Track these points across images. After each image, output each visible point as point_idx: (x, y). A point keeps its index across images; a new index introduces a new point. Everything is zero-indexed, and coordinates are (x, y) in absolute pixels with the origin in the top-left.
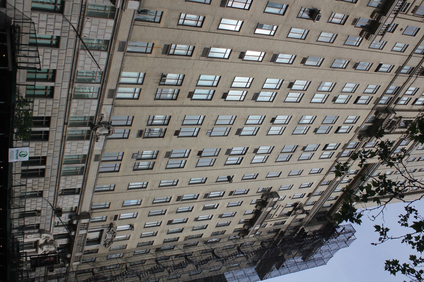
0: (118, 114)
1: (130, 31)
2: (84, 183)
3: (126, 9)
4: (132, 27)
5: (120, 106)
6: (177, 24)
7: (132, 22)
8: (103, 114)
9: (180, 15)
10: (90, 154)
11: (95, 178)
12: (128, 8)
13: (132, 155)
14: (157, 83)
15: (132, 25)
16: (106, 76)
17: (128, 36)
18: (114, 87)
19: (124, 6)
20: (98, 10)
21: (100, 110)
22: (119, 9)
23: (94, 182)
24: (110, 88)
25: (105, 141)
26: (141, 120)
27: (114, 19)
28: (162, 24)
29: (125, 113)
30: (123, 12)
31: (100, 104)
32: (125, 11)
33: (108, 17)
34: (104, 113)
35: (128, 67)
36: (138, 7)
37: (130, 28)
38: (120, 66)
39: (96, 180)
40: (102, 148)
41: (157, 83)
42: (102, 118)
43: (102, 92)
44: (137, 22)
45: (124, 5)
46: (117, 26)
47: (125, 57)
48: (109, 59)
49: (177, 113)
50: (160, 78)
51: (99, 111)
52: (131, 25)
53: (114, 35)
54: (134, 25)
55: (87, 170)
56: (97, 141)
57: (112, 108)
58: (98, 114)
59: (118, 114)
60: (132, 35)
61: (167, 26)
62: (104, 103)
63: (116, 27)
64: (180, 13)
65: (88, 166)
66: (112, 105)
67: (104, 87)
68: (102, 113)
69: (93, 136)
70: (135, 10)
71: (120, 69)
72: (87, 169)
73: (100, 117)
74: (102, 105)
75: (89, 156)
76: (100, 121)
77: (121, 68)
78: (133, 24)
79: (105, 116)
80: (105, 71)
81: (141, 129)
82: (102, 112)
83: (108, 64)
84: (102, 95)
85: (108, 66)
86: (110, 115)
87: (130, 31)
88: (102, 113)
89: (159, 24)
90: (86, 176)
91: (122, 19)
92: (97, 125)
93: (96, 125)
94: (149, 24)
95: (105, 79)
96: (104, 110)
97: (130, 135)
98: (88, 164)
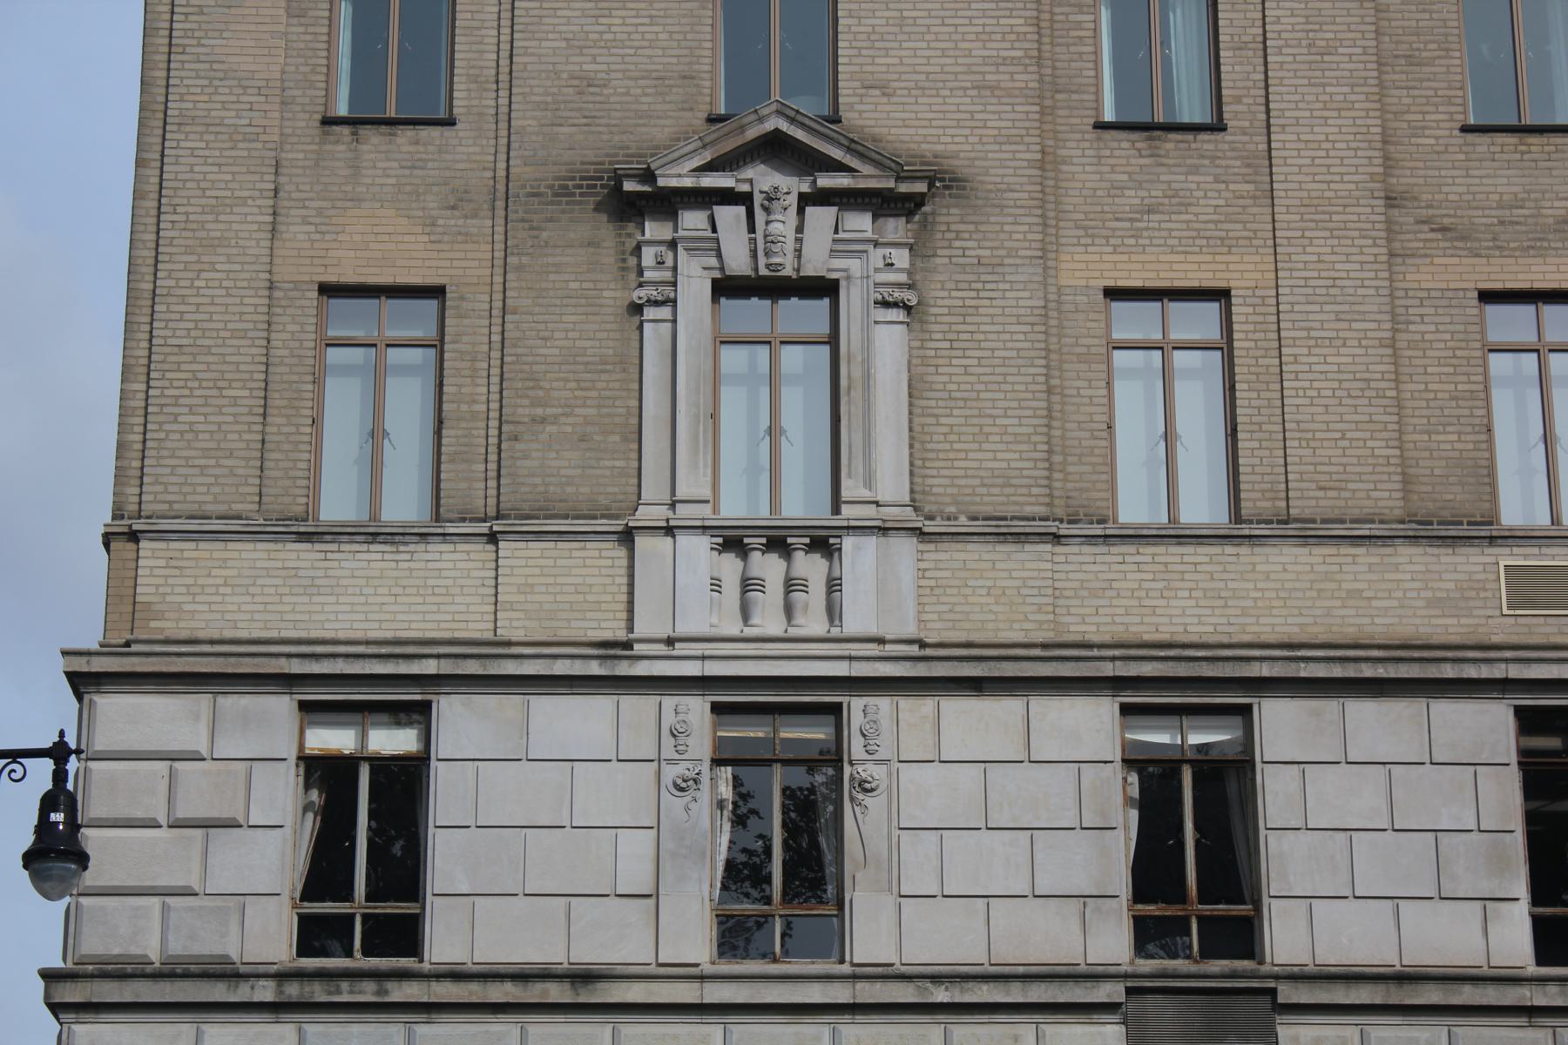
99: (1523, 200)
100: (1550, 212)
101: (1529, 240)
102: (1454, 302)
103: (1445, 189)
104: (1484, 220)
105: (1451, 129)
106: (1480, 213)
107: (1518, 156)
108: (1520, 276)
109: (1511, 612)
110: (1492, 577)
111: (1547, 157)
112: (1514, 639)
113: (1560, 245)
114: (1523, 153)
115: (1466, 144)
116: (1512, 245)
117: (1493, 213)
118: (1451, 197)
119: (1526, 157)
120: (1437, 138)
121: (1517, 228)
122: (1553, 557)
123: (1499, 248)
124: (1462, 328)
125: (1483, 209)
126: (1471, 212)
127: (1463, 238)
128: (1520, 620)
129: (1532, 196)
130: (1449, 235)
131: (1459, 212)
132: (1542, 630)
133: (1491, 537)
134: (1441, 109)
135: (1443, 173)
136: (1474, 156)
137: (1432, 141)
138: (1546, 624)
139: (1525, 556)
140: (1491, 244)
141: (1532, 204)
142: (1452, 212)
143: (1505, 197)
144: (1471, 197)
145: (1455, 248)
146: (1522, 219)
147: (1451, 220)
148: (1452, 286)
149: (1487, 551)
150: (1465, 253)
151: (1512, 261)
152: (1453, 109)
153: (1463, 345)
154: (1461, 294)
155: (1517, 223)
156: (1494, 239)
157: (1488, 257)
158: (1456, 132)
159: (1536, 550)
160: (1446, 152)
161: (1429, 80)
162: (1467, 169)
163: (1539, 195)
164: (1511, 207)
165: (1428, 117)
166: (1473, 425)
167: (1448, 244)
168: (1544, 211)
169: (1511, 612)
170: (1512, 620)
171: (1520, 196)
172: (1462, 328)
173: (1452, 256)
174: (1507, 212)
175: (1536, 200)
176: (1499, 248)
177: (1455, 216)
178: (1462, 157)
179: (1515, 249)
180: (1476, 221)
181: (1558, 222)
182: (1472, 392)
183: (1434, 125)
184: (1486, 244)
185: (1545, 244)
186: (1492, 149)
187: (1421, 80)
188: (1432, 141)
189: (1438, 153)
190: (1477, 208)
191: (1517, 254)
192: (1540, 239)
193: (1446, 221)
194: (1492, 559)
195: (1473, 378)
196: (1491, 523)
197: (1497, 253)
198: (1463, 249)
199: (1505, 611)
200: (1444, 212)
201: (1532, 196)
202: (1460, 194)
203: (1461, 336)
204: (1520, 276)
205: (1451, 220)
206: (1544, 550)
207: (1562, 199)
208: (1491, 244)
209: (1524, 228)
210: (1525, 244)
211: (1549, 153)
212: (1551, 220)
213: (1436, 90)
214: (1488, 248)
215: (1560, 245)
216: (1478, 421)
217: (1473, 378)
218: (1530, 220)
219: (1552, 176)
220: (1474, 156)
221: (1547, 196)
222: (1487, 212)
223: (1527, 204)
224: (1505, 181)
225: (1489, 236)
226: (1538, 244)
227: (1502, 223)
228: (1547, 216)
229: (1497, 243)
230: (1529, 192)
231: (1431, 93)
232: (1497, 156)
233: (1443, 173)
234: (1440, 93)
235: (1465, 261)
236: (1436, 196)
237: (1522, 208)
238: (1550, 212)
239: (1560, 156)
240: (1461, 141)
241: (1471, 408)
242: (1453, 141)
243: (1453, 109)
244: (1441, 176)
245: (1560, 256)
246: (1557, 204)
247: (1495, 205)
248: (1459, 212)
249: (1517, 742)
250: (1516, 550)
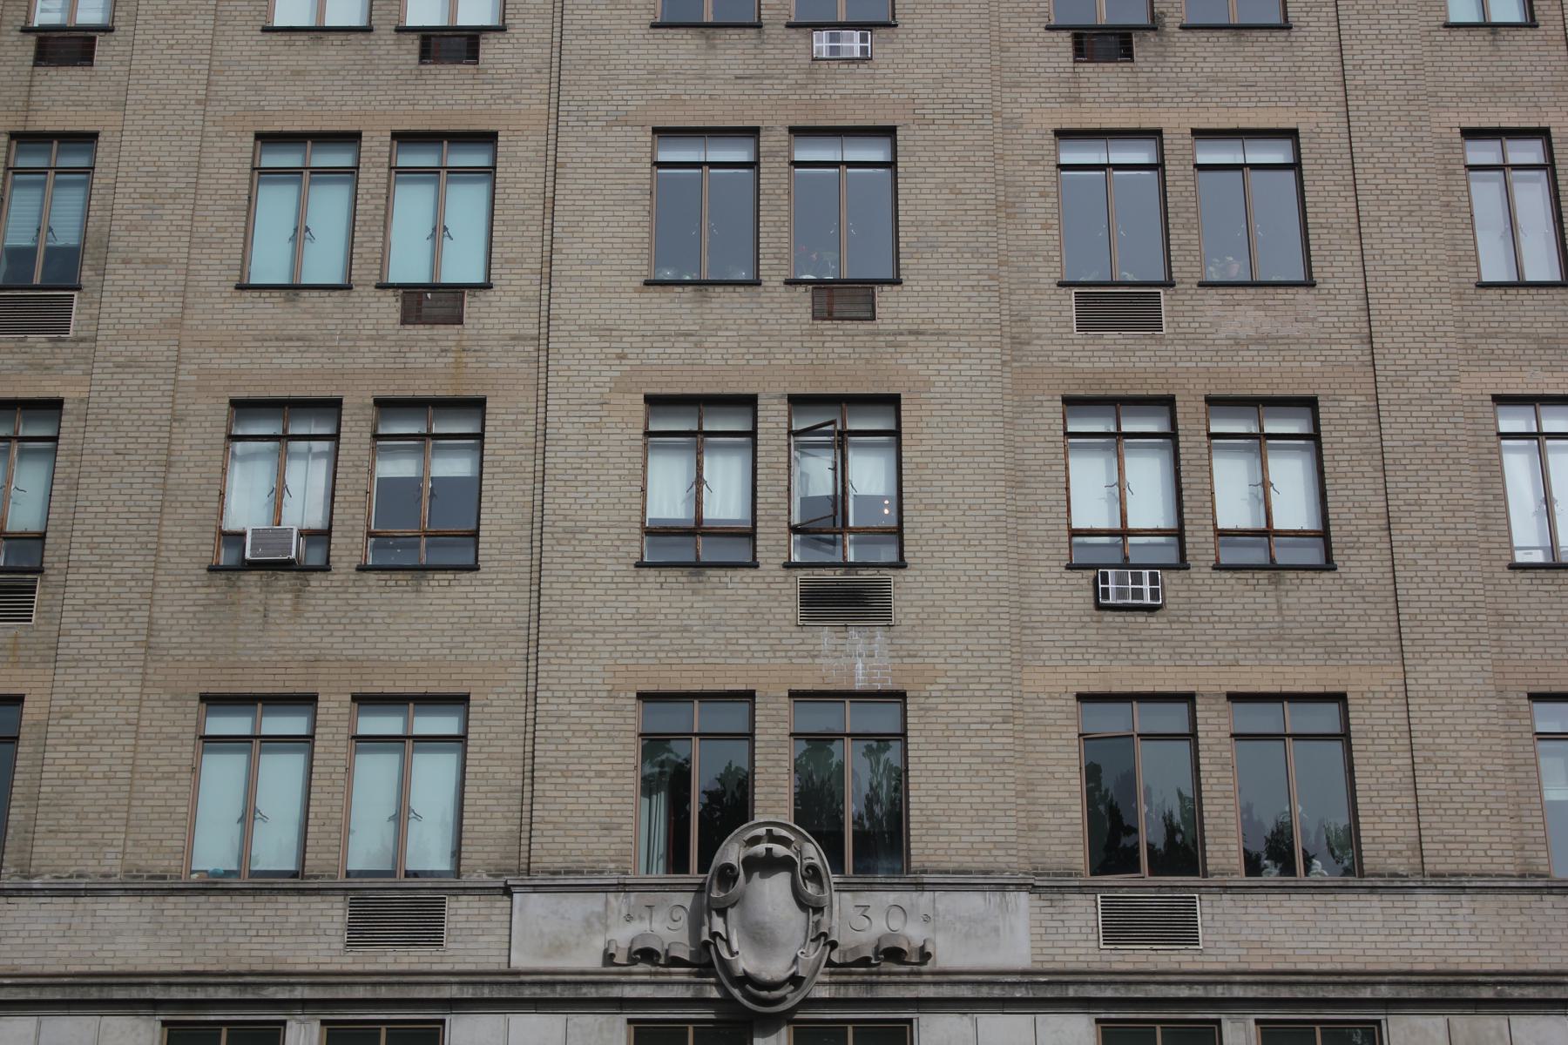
0: (607, 828)
2: (1487, 993)
5: (526, 825)
8: (609, 958)
10: (1071, 992)
11: (1427, 904)
13: (1109, 617)
14: (298, 593)
16: (200, 994)
18: (334, 914)
21: (580, 979)
23: (1490, 902)
24: (338, 939)
25: (920, 887)
26: (686, 629)
29: (600, 774)
31: (486, 993)
34: (599, 944)
35: (136, 843)
38: (124, 903)
39: (1452, 885)
40: (1023, 898)
41: (298, 593)
42: (648, 955)
43: (360, 993)
47: (36, 883)
48: (33, 994)
49: (622, 357)
50: (252, 577)
51: (559, 992)
55: (1199, 992)
56: (925, 956)
57: (536, 889)
58: (592, 992)
59: (607, 828)
62: (494, 962)
65: (1238, 992)
66: (507, 891)
67: (299, 993)
68: (592, 961)
69: (852, 993)
71: (149, 901)
72: (1285, 993)
73: (642, 967)
74: (513, 977)
75: (1109, 993)
76: (676, 962)
77: (141, 892)
79: (624, 935)
80: (154, 1005)
81: (790, 607)
82: (588, 959)
83: (77, 994)
84: (384, 993)
85: (94, 994)
86: (622, 888)
88: (592, 961)
90: (1385, 992)
92: (719, 985)
93: (714, 993)
95: (224, 993)
96: (559, 948)
97: (859, 685)
98: (1219, 992)
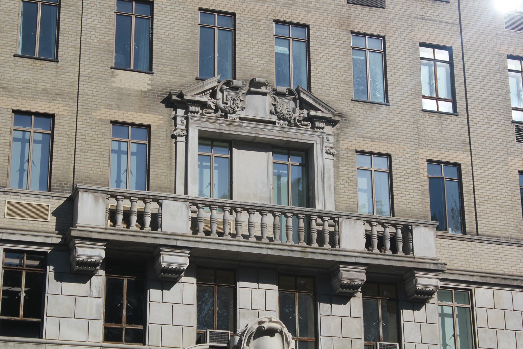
1: (496, 243)
3: (439, 262)
4: (485, 238)
6: (454, 118)
7: (472, 240)
9: (427, 114)
12: (433, 255)
15: (480, 237)
17: (512, 244)
19: (432, 267)
20: (454, 335)
22: (442, 280)
27: (471, 290)
28: (462, 158)
30: (447, 267)
32: (443, 262)
33: (470, 306)
36: (427, 229)
37: (489, 242)
44: (470, 226)
45: (427, 266)
46: (488, 280)
52: (480, 241)
53: (515, 283)
54: (478, 235)
60: (508, 234)
61: (464, 142)
63: (493, 281)
64: (422, 113)
70: (438, 237)
78: (475, 237)
87: (497, 241)
89: (462, 167)
91: (468, 269)
94: (468, 193)
99: (32, 81)
100: (40, 86)
101: (32, 95)
102: (3, 112)
103: (6, 74)
104: (18, 87)
105: (11, 55)
106: (16, 84)
107: (32, 67)
108: (27, 106)
109: (8, 217)
110: (3, 205)
111: (41, 68)
112: (8, 226)
113: (42, 98)
114: (34, 66)
115: (15, 61)
116: (26, 96)
117: (21, 84)
118: (7, 78)
119: (35, 67)
120: (5, 57)
121: (29, 90)
122: (25, 200)
123: (21, 96)
124: (5, 121)
125: (18, 83)
126: (13, 83)
127: (9, 92)
128: (10, 220)
129: (35, 80)
130: (5, 90)
131: (9, 83)
132: (17, 224)
133: (4, 192)
134: (8, 48)
135: (6, 69)
136: (17, 65)
137: (4, 58)
138: (19, 222)
139: (15, 199)
140: (19, 95)
141: (34, 83)
142: (7, 82)
143: (26, 80)
144: (14, 78)
145: (7, 94)
146: (30, 88)
147: (7, 85)
148: (4, 107)
149: (3, 196)
150: (10, 96)
151: (25, 101)
152: (12, 48)
153: (5, 127)
154: (6, 110)
155: (29, 89)
156: (20, 93)
157: (17, 99)
158: (12, 56)
159: (19, 197)
160: (8, 62)
161: (5, 38)
162: (14, 69)
163: (37, 81)
164: (27, 83)
165: (3, 50)
166: (4, 154)
167: (4, 93)
168: (38, 86)
169: (8, 217)
170: (8, 220)
171: (31, 80)
172: (5, 121)
173: (5, 97)
174: (26, 85)
175: (36, 82)
176: (21, 96)
177: (8, 84)
178: (13, 65)
179: (26, 97)
180: (15, 86)
181: (42, 90)
182: (5, 143)
183: (5, 53)
184: (17, 94)
185: (37, 97)
186: (24, 63)
187: (3, 38)
188: (4, 58)
189: (5, 62)
190: (16, 82)
191: (27, 99)
192: (36, 95)
193: (5, 85)
194: (4, 199)
195: (6, 138)
196: (5, 187)
197: (20, 98)
198: (9, 95)
199: (6, 217)
200: (4, 82)
201: (35, 80)
202: (11, 77)
203: (4, 124)
204: (27, 106)
205: (7, 85)
206: (22, 197)
207: (44, 83)
208: (19, 95)
209: (30, 91)
210: (30, 96)
211: (42, 67)
212: (40, 89)
213: (7, 41)
214: (18, 96)
215: (42, 98)
216: (6, 153)
217: (6, 138)
218: (33, 88)
219: (42, 75)
220: (17, 65)
221: (40, 81)
222: (19, 84)
223: (33, 83)
224: (26, 74)
225: (19, 92)
226: (35, 96)
227: (23, 88)
228: (39, 88)
229: (21, 95)
230: (34, 79)
231: (6, 42)
232: (25, 66)
233: (6, 69)
234: (8, 43)
235: (9, 99)
236: (2, 77)
237: (31, 84)
238: (40, 86)
239: (46, 68)
240: (13, 59)
241: (4, 148)
242: (11, 59)
243: (12, 48)
244: (5, 70)
245: (41, 101)
246: (42, 84)
247: (22, 82)
248: (9, 83)
249: (3, 260)
250: (12, 197)
